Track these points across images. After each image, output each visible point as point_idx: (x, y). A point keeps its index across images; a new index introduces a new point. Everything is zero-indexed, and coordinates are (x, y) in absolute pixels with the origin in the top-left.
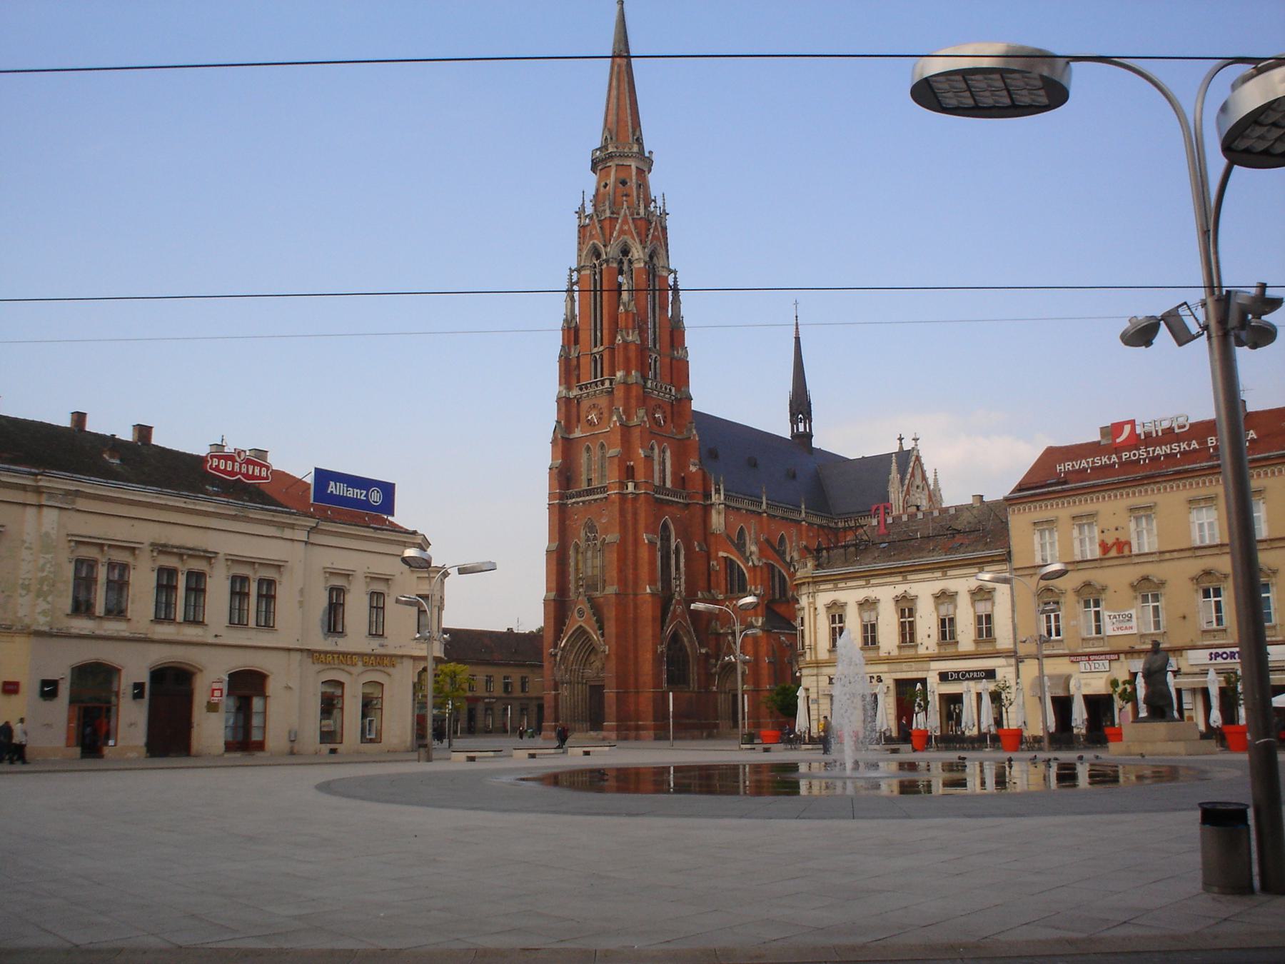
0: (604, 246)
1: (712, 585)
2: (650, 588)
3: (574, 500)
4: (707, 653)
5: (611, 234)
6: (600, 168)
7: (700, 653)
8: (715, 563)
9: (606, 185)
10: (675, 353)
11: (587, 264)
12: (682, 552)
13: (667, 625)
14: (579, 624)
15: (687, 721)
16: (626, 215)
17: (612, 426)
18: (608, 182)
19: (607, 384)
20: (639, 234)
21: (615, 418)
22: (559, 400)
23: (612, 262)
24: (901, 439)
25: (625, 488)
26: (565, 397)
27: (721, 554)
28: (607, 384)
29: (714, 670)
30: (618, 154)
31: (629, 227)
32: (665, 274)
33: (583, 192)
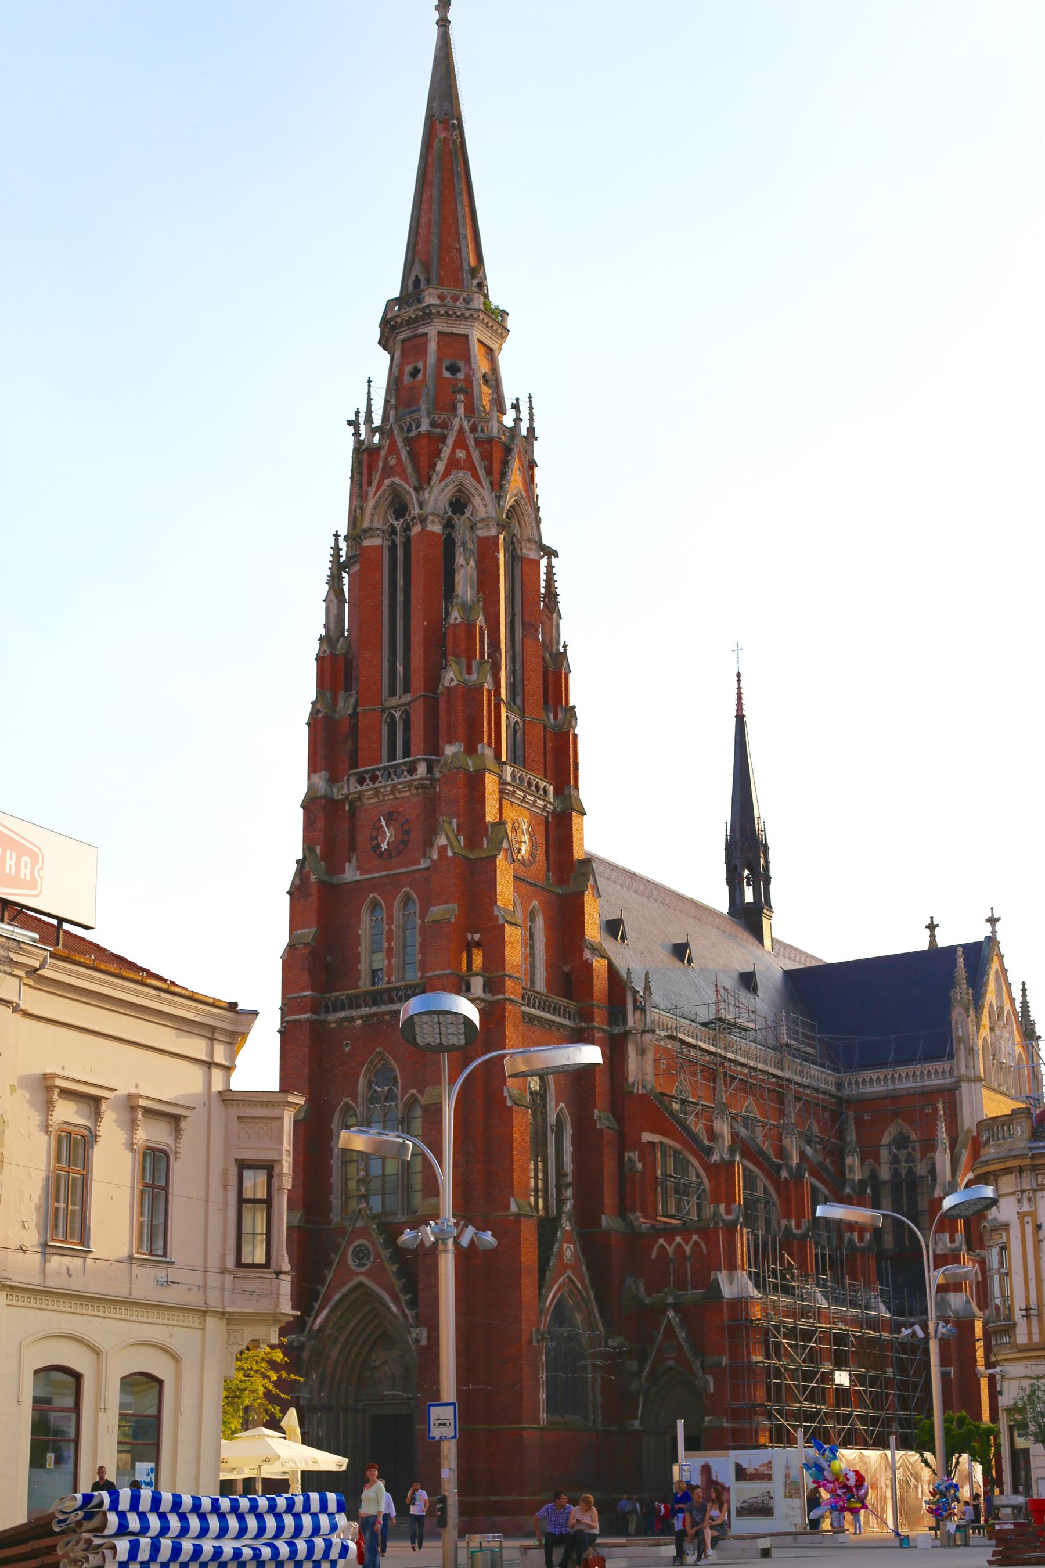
0: (415, 489)
2: (517, 1205)
3: (342, 1014)
5: (433, 467)
6: (402, 337)
8: (634, 1155)
9: (415, 373)
10: (551, 716)
11: (375, 525)
12: (568, 1132)
14: (356, 1280)
16: (461, 430)
17: (435, 857)
18: (420, 365)
19: (422, 770)
20: (489, 472)
21: (442, 841)
22: (309, 805)
23: (433, 522)
24: (932, 927)
25: (464, 988)
26: (325, 797)
27: (646, 1137)
28: (422, 770)
30: (442, 312)
31: (469, 456)
32: (533, 555)
33: (369, 381)
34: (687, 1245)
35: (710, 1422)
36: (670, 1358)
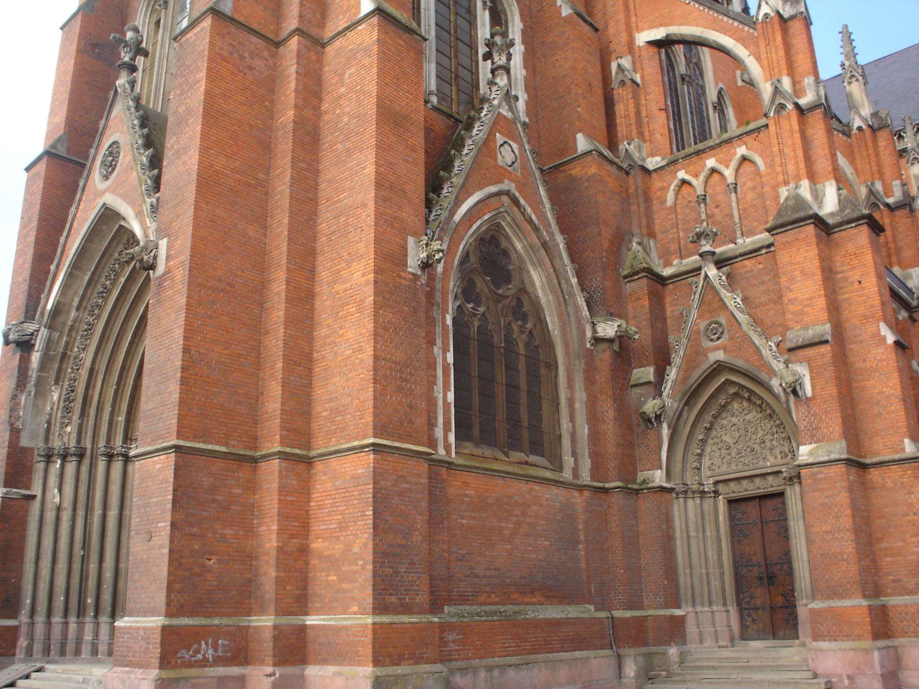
1: (621, 130)
4: (622, 339)
7: (597, 340)
13: (457, 181)
15: (552, 612)
27: (643, 37)
29: (651, 406)
34: (727, 167)
35: (811, 453)
36: (717, 348)
